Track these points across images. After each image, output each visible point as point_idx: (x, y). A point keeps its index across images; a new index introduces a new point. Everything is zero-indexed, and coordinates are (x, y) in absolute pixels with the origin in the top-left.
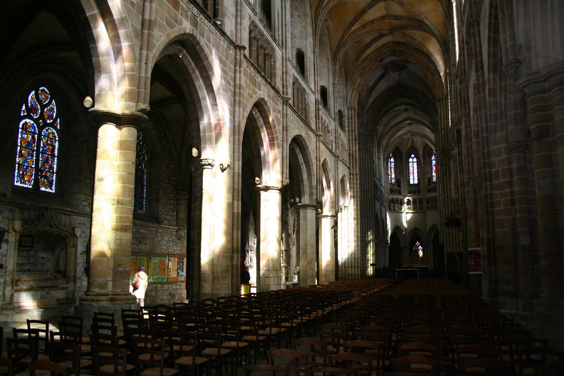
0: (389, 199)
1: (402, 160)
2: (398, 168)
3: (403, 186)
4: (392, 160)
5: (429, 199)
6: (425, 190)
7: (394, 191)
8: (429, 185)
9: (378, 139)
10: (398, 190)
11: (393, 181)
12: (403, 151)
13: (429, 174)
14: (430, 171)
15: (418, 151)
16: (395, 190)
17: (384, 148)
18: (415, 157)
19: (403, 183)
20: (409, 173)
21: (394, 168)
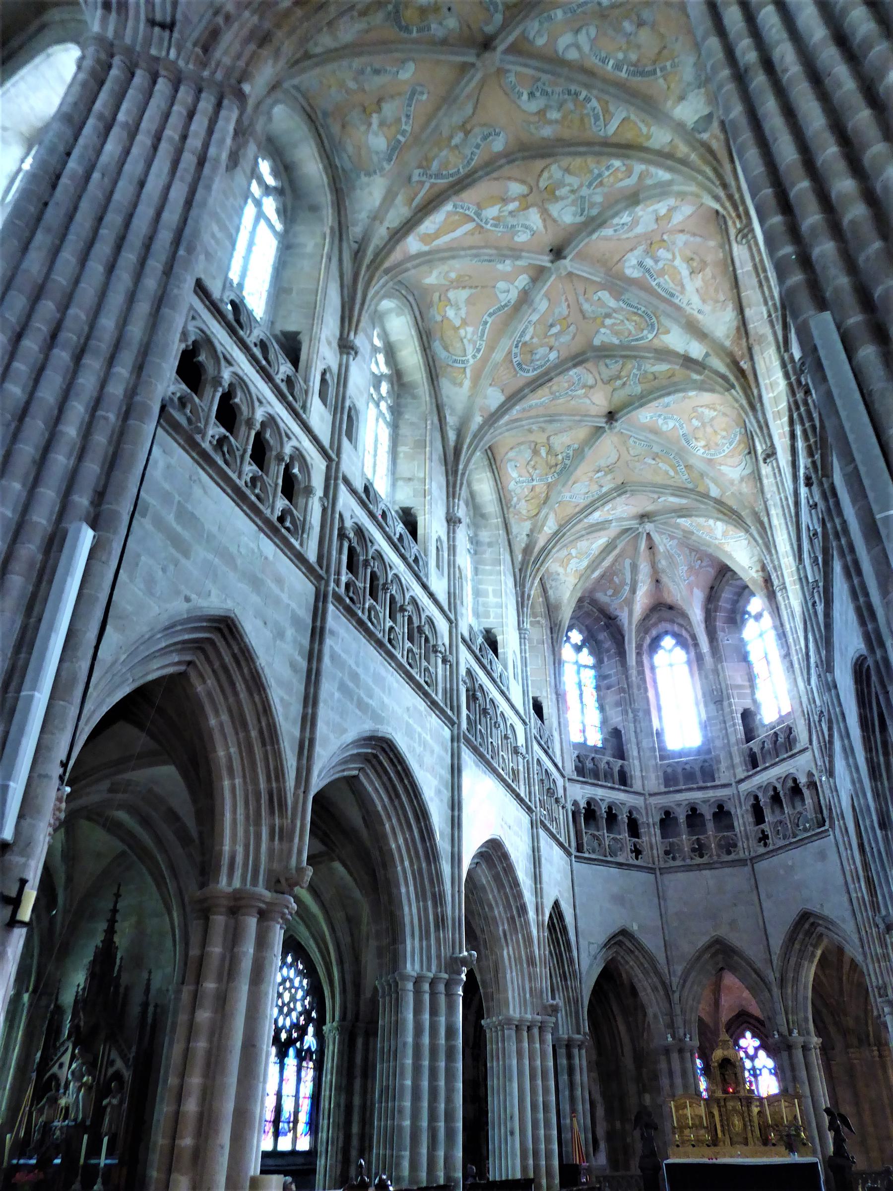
0: (575, 803)
1: (622, 653)
2: (608, 688)
3: (635, 753)
4: (586, 657)
5: (760, 795)
6: (737, 760)
7: (595, 774)
8: (749, 735)
10: (616, 769)
11: (595, 738)
12: (624, 616)
13: (740, 696)
14: (747, 684)
15: (684, 616)
16: (602, 765)
17: (519, 557)
18: (681, 642)
19: (633, 740)
20: (659, 709)
21: (598, 688)
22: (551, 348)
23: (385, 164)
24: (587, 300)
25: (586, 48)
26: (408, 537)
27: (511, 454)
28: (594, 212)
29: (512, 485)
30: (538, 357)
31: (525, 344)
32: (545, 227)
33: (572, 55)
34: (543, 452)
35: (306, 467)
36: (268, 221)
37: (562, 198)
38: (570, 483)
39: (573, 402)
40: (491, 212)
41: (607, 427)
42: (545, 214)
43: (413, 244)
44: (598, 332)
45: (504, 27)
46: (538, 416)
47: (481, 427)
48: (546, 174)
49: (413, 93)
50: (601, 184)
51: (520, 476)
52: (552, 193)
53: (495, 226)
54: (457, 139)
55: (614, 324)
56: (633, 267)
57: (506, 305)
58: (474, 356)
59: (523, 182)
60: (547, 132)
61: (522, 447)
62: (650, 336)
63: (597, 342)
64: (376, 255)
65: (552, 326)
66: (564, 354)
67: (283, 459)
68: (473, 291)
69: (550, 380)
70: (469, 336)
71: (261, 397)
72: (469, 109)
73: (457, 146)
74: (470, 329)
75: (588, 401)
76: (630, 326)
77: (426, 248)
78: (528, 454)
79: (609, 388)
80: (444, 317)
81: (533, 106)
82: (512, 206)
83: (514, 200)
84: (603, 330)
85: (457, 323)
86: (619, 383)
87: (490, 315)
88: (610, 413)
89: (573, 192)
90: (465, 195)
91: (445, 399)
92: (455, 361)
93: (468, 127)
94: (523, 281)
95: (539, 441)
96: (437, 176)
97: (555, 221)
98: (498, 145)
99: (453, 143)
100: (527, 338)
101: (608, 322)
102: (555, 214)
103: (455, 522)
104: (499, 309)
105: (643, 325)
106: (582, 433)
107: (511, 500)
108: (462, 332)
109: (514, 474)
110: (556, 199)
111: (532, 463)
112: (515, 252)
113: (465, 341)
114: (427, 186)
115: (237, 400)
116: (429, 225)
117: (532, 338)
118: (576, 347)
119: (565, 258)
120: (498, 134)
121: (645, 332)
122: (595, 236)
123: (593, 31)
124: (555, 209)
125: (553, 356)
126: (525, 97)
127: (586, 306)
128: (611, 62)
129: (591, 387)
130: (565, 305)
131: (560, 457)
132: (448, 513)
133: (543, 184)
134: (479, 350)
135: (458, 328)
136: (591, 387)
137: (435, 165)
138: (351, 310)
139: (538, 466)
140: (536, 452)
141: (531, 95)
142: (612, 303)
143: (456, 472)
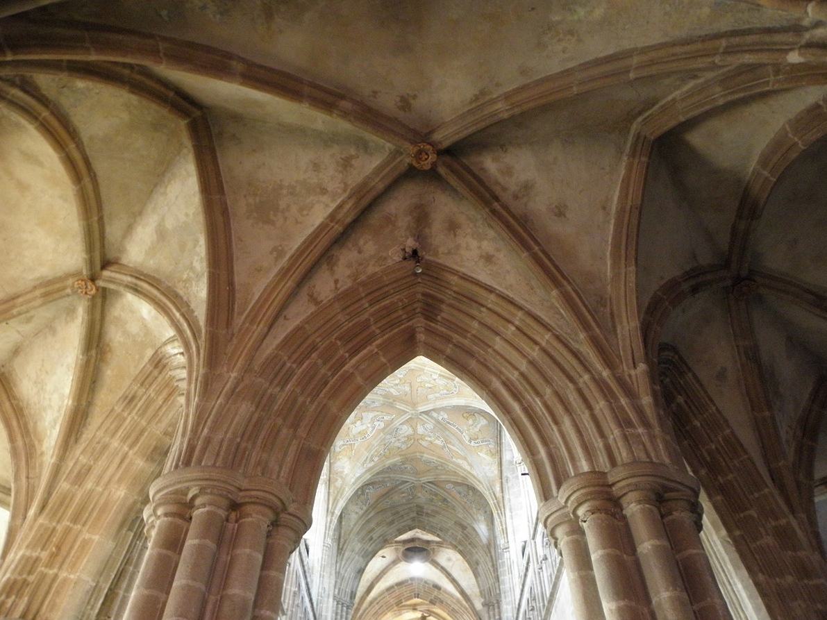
22: (435, 380)
32: (417, 424)
37: (405, 437)
42: (415, 430)
52: (409, 438)
55: (395, 380)
65: (430, 388)
82: (429, 439)
89: (399, 440)
100: (445, 391)
101: (397, 382)
102: (410, 429)
110: (408, 437)
124: (410, 431)
127: (407, 389)
142: (392, 390)
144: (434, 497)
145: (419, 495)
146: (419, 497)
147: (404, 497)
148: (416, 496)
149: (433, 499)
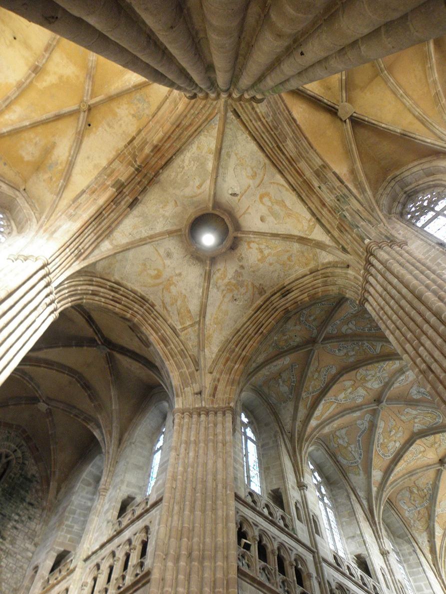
9: (366, 507)
17: (429, 557)
23: (290, 396)
24: (402, 415)
25: (354, 328)
26: (365, 576)
27: (399, 497)
28: (386, 380)
29: (407, 514)
30: (390, 448)
31: (382, 444)
33: (349, 331)
34: (415, 491)
35: (304, 562)
36: (250, 439)
38: (437, 503)
39: (418, 462)
40: (342, 396)
41: (442, 468)
42: (365, 388)
43: (313, 423)
44: (414, 426)
45: (318, 333)
46: (404, 475)
47: (378, 492)
48: (358, 374)
49: (292, 366)
50: (384, 370)
51: (409, 507)
52: (364, 380)
53: (346, 400)
54: (316, 376)
55: (420, 421)
56: (416, 394)
57: (365, 430)
58: (360, 458)
59: (350, 380)
60: (352, 360)
61: (403, 491)
62: (441, 421)
63: (416, 430)
64: (299, 435)
65: (390, 432)
66: (402, 441)
67: (293, 565)
68: (347, 429)
69: (402, 456)
70: (353, 450)
71: (274, 536)
72: (317, 364)
73: (317, 378)
74: (352, 446)
75: (426, 459)
76: (428, 419)
77: (319, 422)
78: (408, 494)
79: (433, 449)
80: (339, 445)
81: (342, 353)
82: (349, 391)
83: (349, 388)
84: (416, 425)
85: (346, 445)
86: (436, 445)
87: (359, 437)
88: (440, 460)
90: (328, 395)
91: (355, 484)
92: (352, 463)
93: (319, 370)
94: (368, 417)
95: (410, 485)
96: (313, 392)
97: (371, 389)
98: (334, 371)
99: (315, 378)
101: (416, 420)
102: (370, 387)
103: (386, 554)
104: (362, 433)
105: (434, 417)
106: (432, 473)
107: (410, 523)
108: (349, 448)
109: (406, 508)
110: (367, 381)
111: (412, 498)
112: (359, 408)
113: (353, 452)
114: (310, 397)
115: (264, 542)
116: (317, 413)
117: (384, 440)
118: (406, 436)
119: (382, 402)
120: (332, 367)
121: (437, 420)
122: (392, 389)
123: (354, 322)
124: (369, 385)
125: (398, 445)
126: (337, 351)
127: (403, 418)
128: (366, 329)
129: (424, 451)
130: (392, 421)
131: (425, 491)
132: (380, 549)
133: (359, 378)
134: (361, 455)
135: (347, 447)
136: (424, 451)
137: (311, 389)
138: (298, 466)
139: (416, 499)
140: (411, 492)
141: (339, 350)
142: (414, 412)
143: (375, 523)
144: (286, 337)
145: (298, 327)
146: (295, 326)
147: (310, 316)
148: (300, 323)
149: (284, 335)
